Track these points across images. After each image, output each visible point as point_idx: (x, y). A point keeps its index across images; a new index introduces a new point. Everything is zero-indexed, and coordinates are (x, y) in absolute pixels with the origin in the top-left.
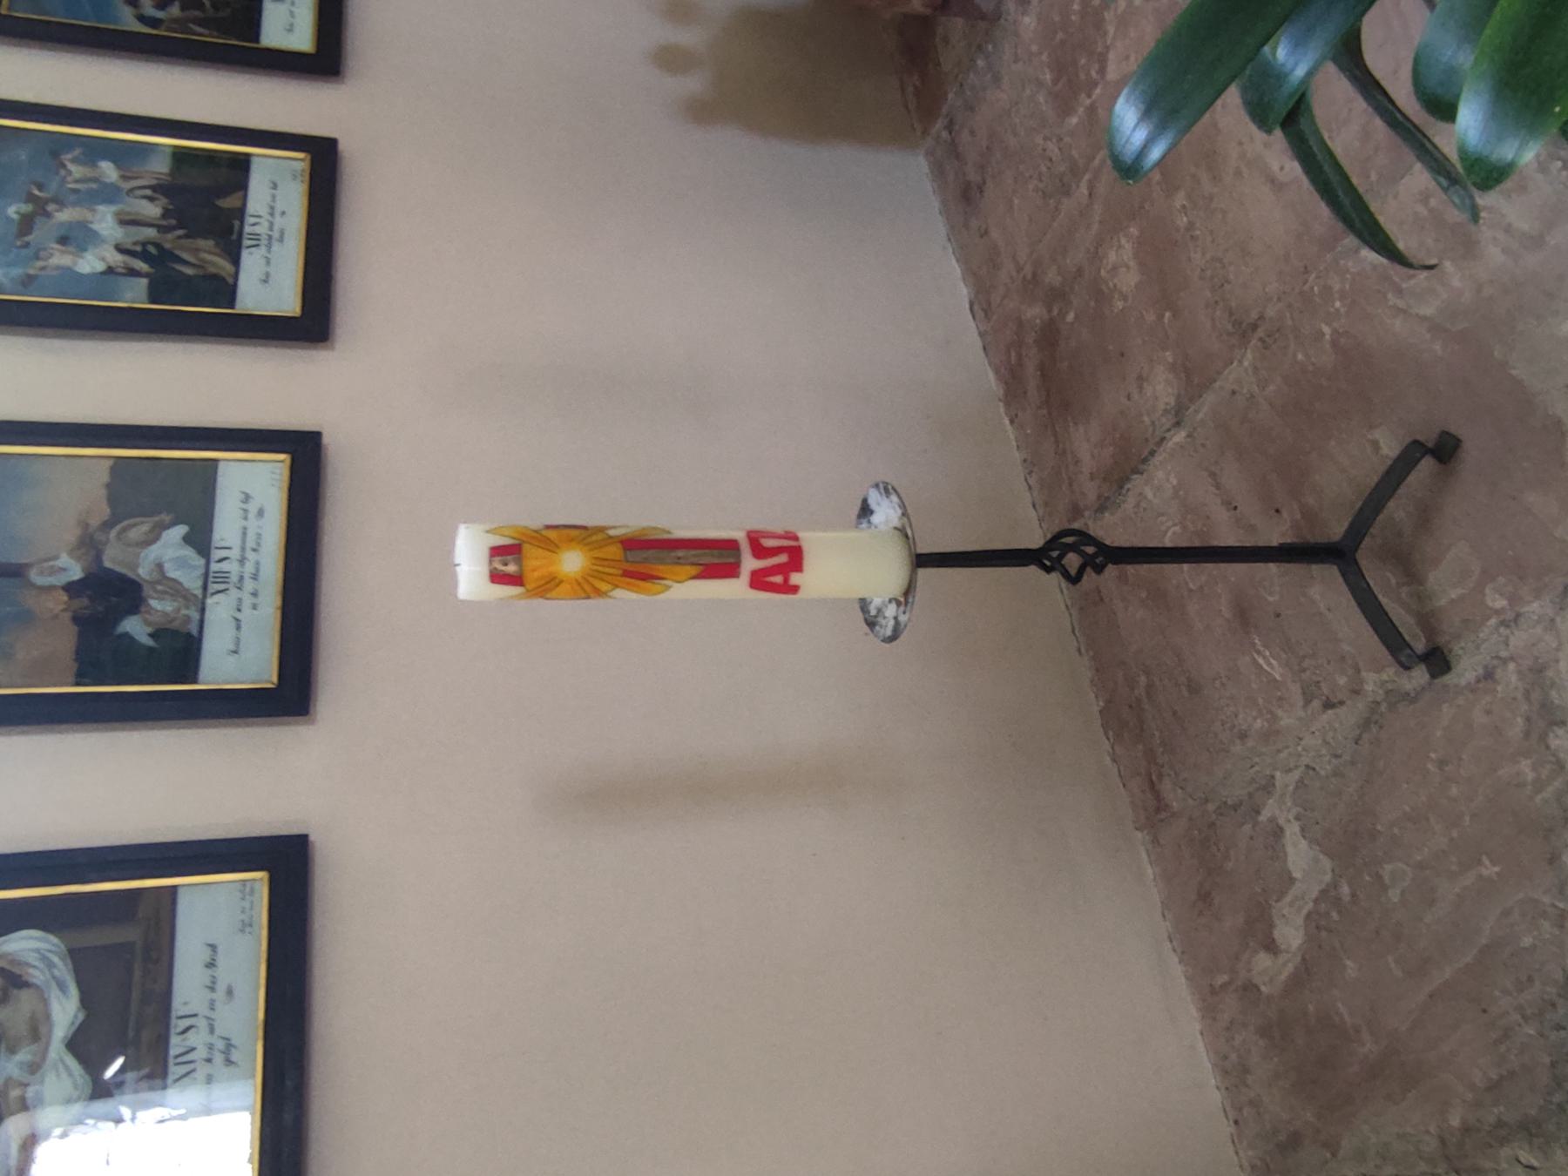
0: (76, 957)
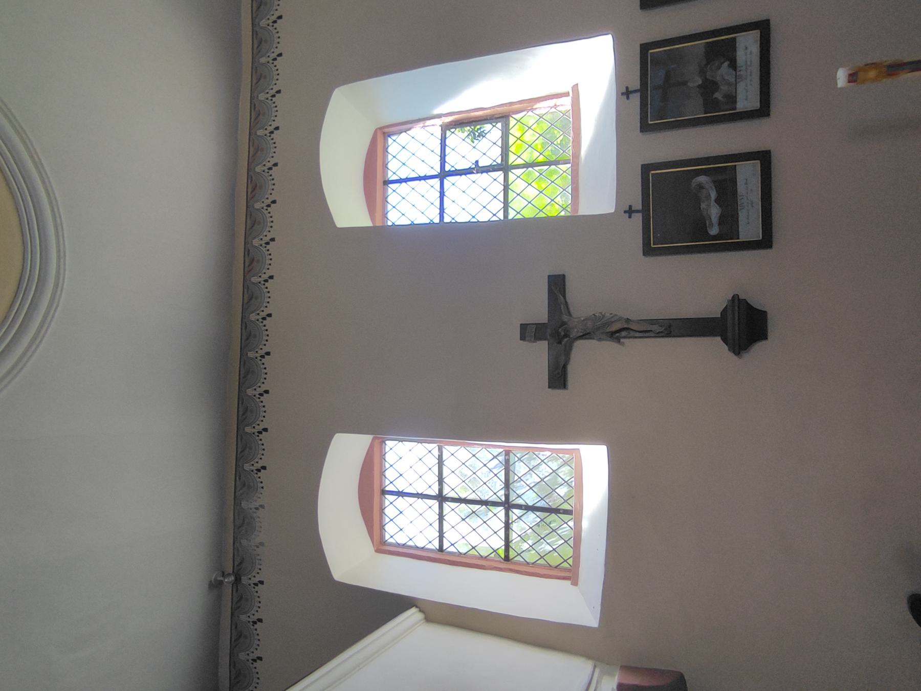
0: (714, 182)
